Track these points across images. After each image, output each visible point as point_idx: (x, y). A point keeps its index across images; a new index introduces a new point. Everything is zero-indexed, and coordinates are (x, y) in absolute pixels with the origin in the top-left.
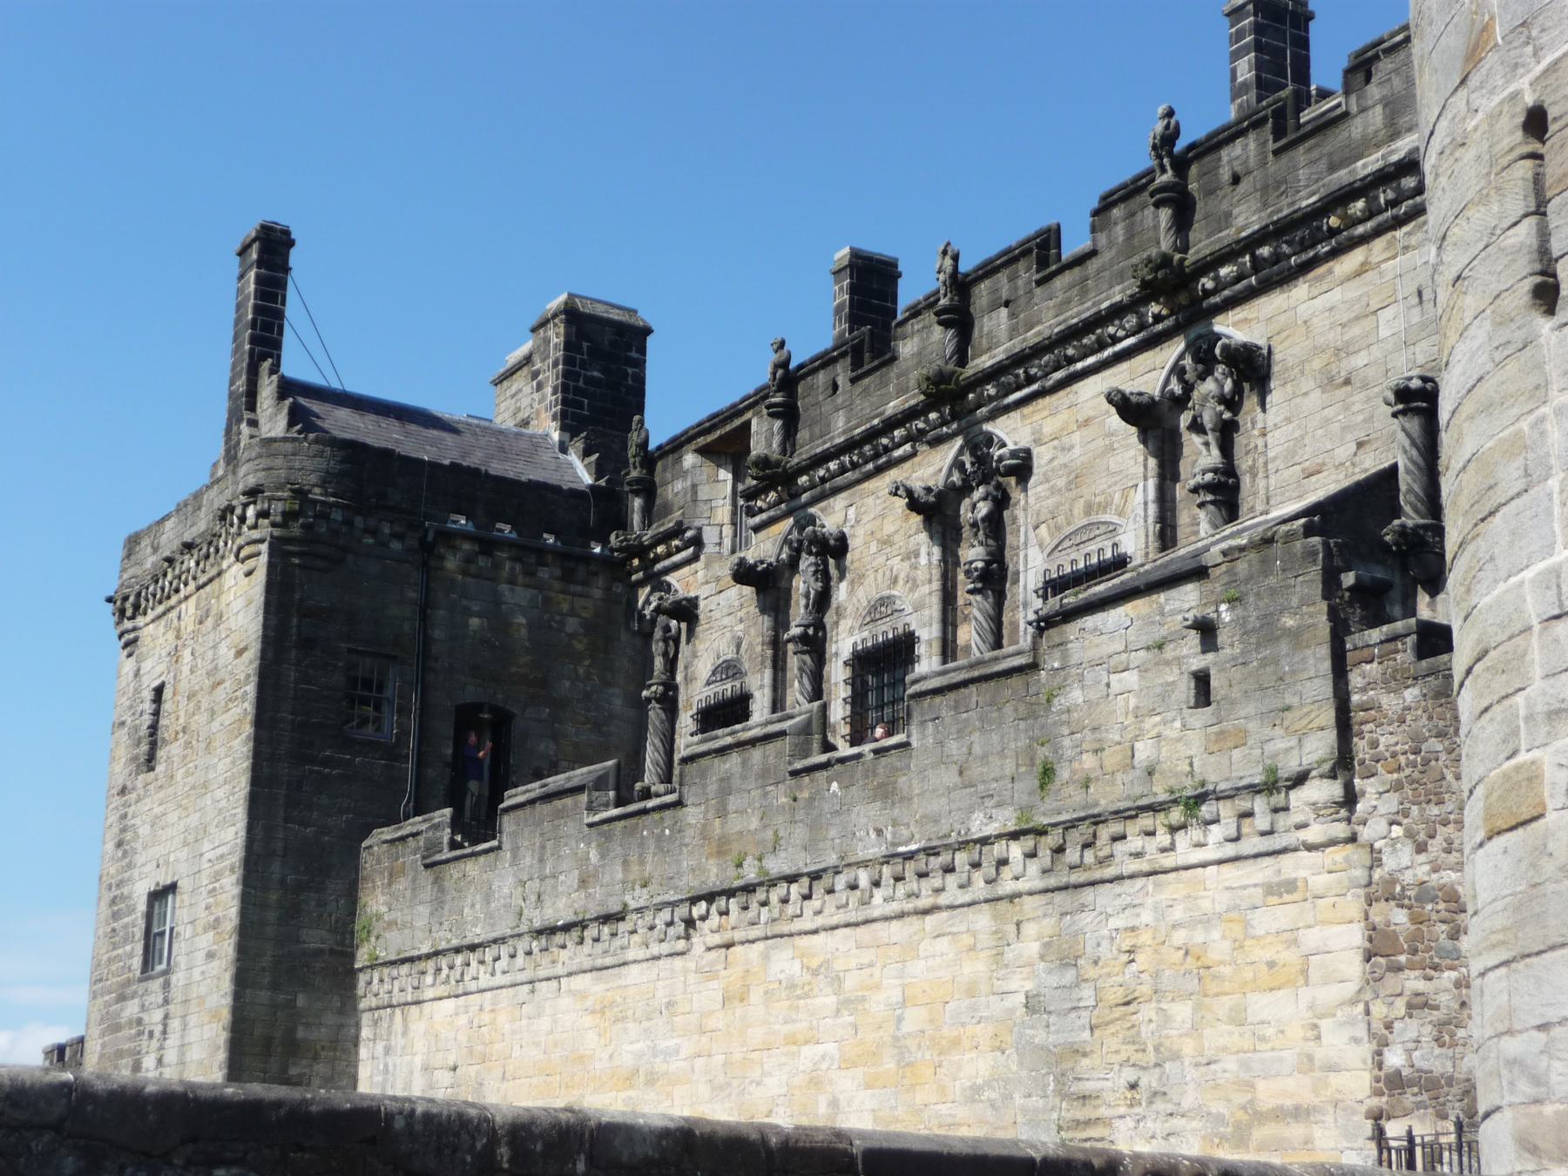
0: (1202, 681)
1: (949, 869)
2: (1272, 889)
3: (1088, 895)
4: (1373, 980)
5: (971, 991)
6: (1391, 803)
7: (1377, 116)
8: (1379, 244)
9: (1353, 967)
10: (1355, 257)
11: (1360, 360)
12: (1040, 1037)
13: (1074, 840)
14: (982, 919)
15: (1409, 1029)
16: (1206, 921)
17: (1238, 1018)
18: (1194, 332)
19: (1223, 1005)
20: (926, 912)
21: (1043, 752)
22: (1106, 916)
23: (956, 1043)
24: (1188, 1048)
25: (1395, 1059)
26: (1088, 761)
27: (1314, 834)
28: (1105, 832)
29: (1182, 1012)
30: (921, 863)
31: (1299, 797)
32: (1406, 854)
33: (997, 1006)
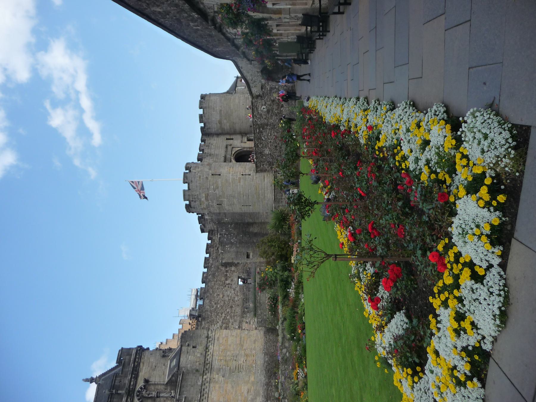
0: (194, 347)
1: (204, 390)
2: (218, 340)
3: (213, 366)
4: (229, 329)
5: (220, 387)
6: (213, 326)
7: (128, 357)
8: (142, 360)
9: (228, 331)
10: (141, 364)
11: (154, 364)
12: (228, 375)
13: (206, 367)
14: (212, 385)
15: (234, 324)
16: (219, 349)
17: (230, 346)
18: (135, 395)
19: (229, 347)
20: (208, 397)
21: (194, 371)
22: (216, 364)
23: (226, 391)
24: (232, 352)
25: (237, 327)
26: (197, 364)
27: (214, 334)
28: (207, 362)
29: (228, 353)
30: (202, 394)
31: (209, 336)
32: (218, 324)
33: (223, 382)
